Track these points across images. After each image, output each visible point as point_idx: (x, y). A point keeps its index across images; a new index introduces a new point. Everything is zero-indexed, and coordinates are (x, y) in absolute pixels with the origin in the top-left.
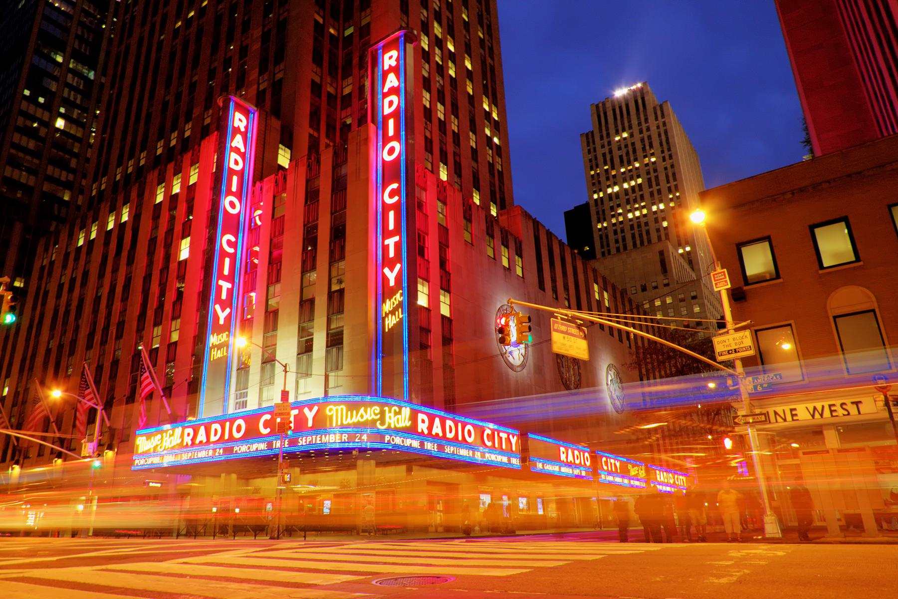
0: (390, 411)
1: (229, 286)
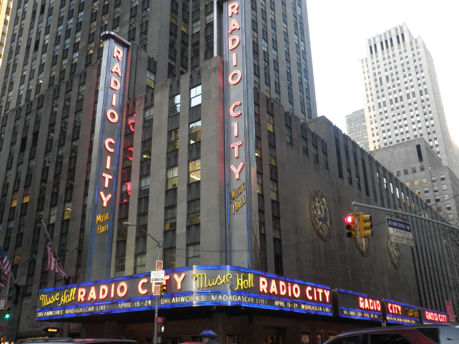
0: (240, 277)
1: (111, 177)
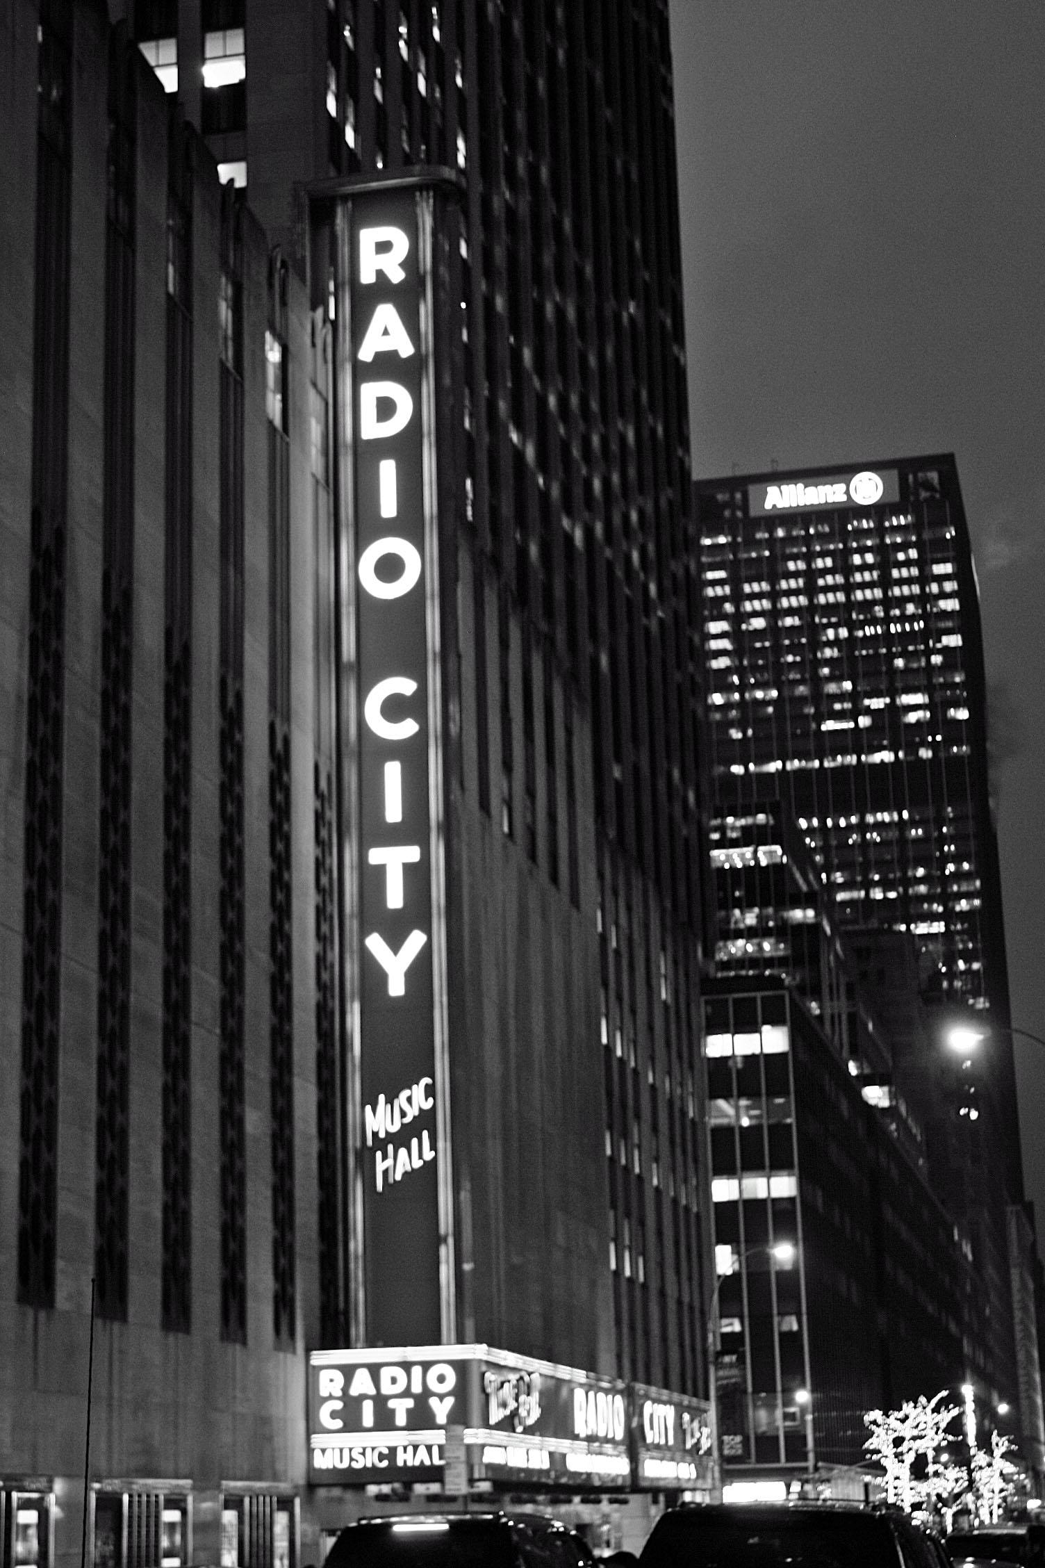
1: (412, 854)
